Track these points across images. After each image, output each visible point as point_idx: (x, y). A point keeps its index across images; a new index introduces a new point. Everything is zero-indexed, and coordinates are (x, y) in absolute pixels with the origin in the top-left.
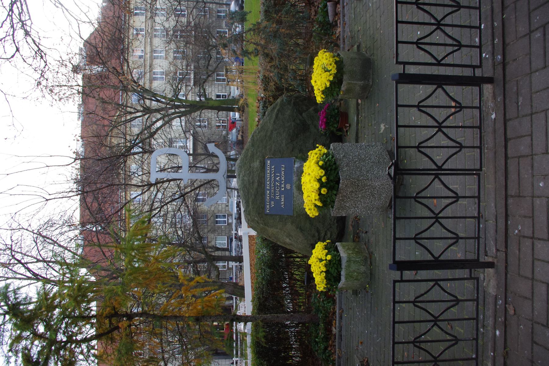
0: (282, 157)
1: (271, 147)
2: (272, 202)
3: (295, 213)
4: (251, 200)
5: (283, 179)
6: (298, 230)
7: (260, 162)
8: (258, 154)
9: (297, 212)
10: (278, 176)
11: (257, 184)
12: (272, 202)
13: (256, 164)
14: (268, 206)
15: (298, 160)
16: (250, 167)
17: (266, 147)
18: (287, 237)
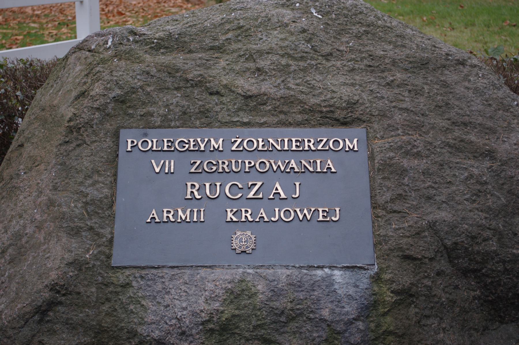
0: (375, 206)
1: (418, 155)
2: (171, 165)
3: (121, 277)
4: (178, 59)
5: (278, 214)
6: (47, 295)
7: (352, 105)
8: (384, 92)
9: (127, 285)
10: (289, 188)
11: (254, 90)
12: (171, 165)
13: (337, 86)
14: (152, 143)
15: (364, 282)
16: (328, 56)
17: (418, 127)
18: (18, 236)
